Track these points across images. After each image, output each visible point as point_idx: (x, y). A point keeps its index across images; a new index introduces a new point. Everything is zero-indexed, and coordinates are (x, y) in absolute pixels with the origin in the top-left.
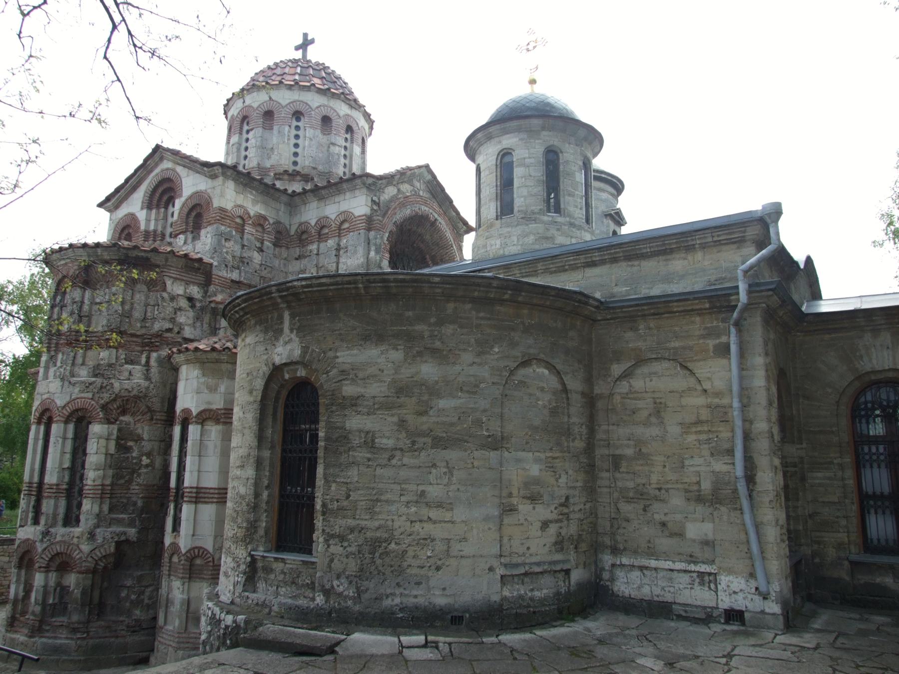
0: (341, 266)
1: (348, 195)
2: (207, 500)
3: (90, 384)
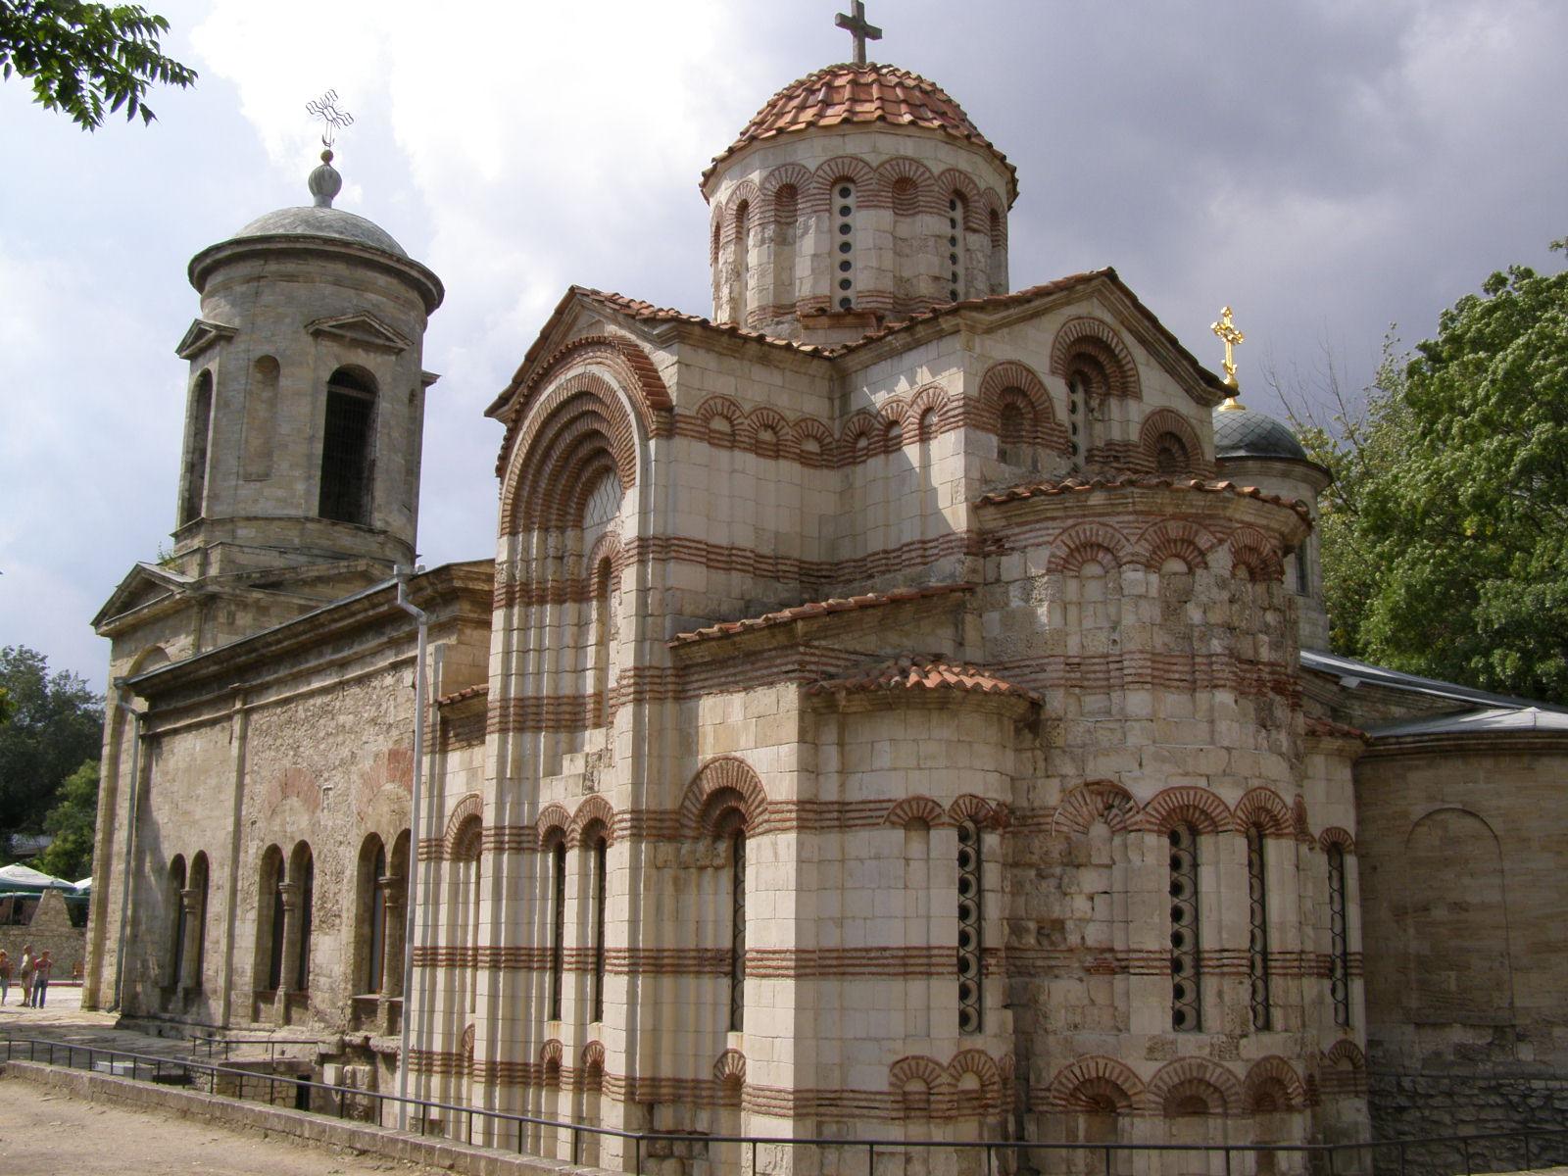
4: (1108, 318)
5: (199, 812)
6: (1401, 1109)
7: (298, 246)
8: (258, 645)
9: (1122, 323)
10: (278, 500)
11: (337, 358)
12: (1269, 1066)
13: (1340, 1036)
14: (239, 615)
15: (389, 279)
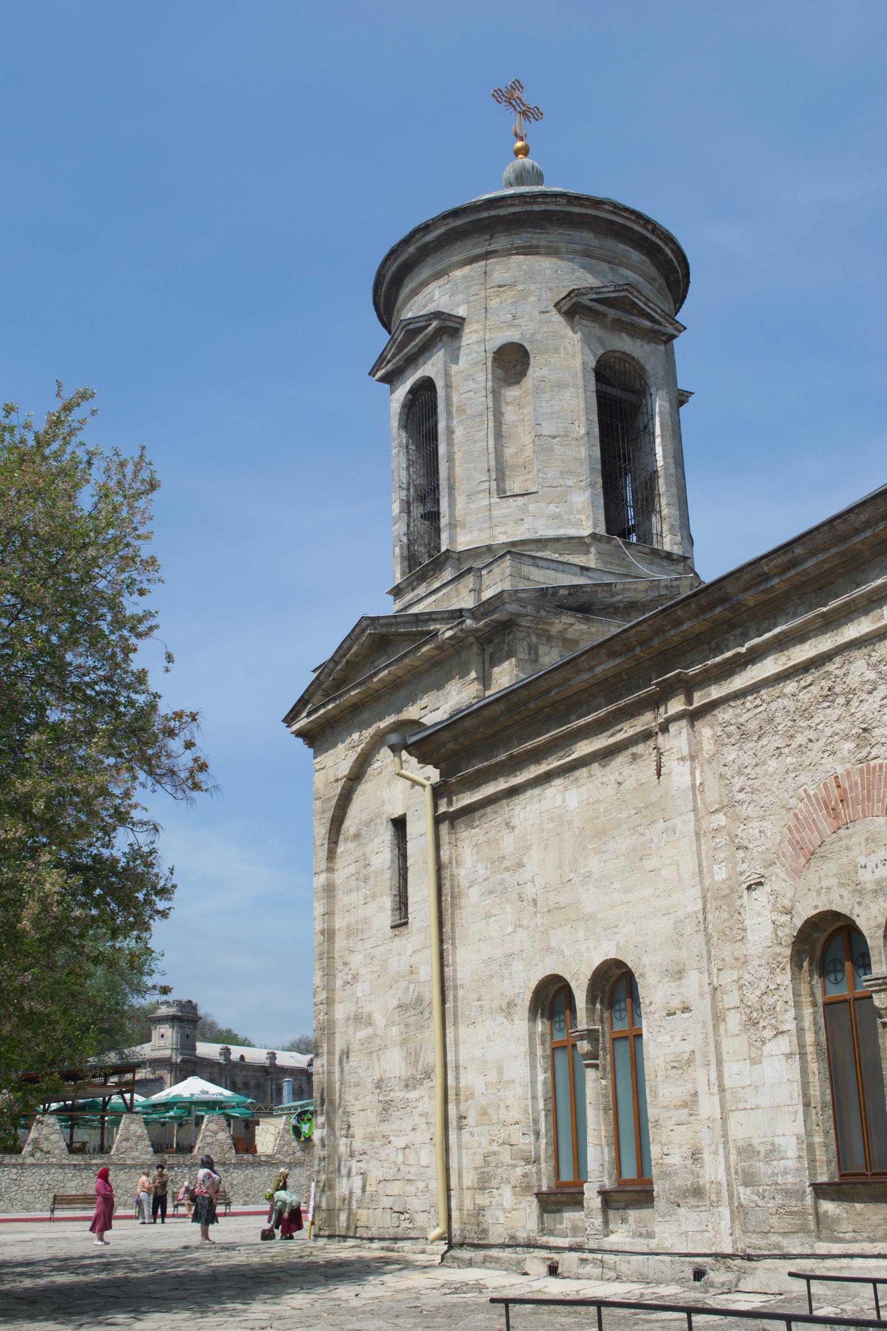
5: (589, 900)
7: (536, 208)
8: (731, 589)
10: (552, 517)
11: (601, 342)
14: (542, 649)
15: (644, 258)
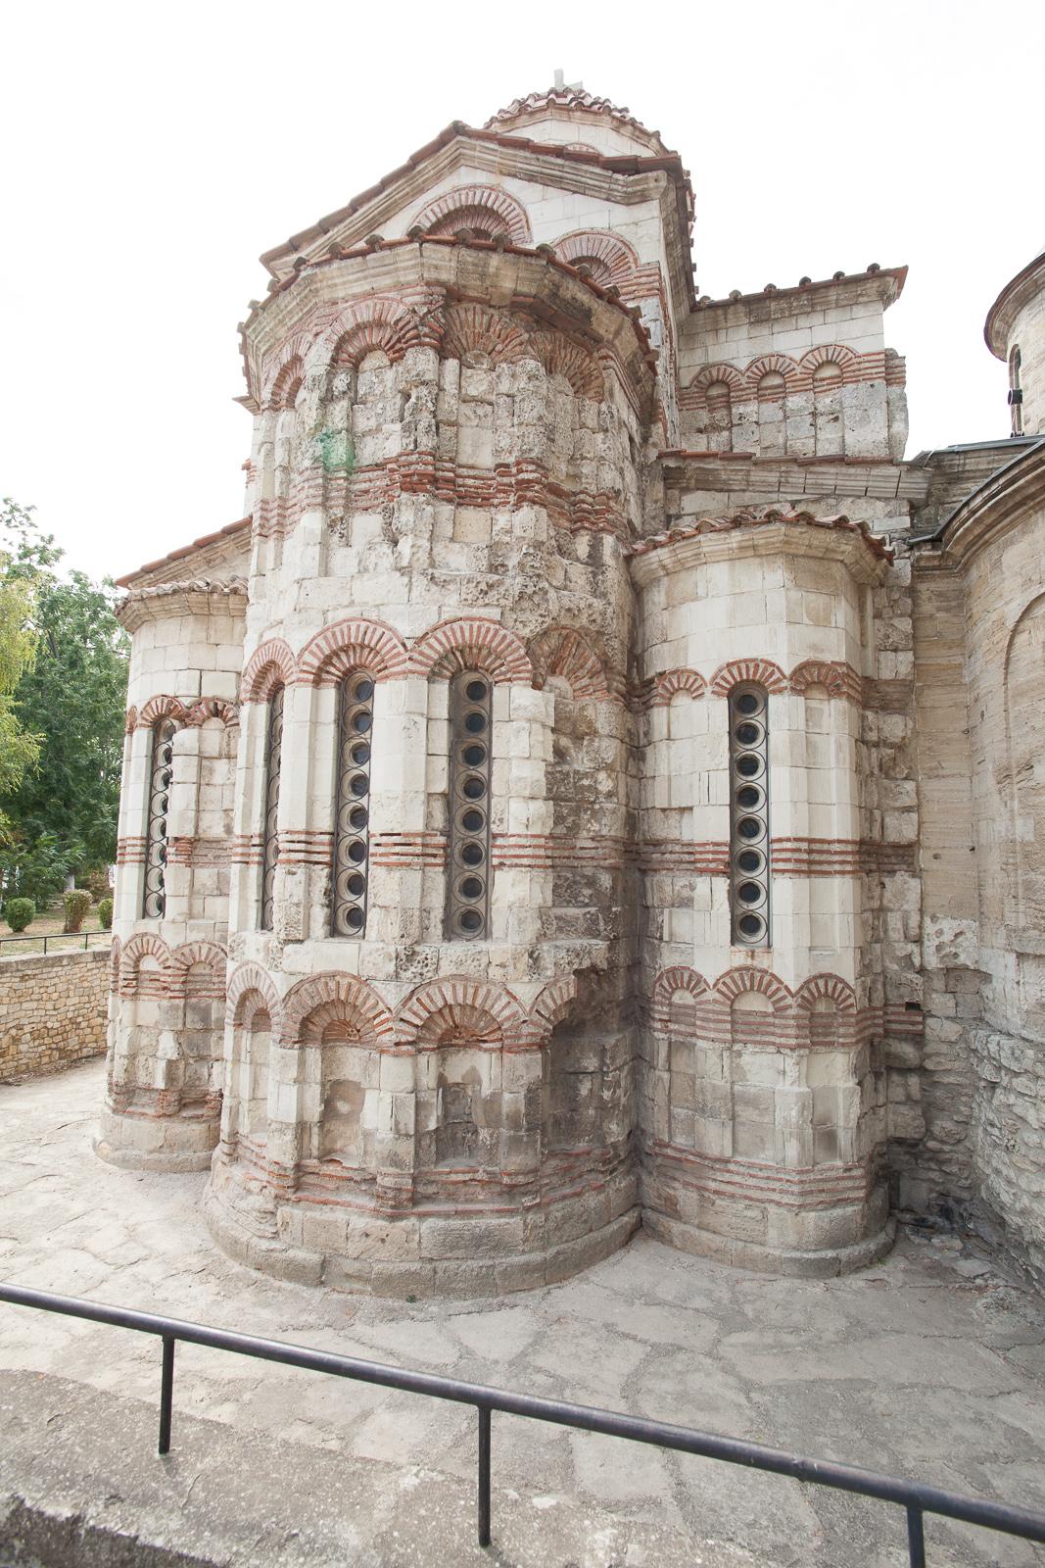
0: (819, 447)
1: (833, 315)
2: (825, 867)
3: (491, 586)
4: (482, 178)
6: (993, 1086)
9: (501, 173)
12: (332, 985)
13: (739, 957)
